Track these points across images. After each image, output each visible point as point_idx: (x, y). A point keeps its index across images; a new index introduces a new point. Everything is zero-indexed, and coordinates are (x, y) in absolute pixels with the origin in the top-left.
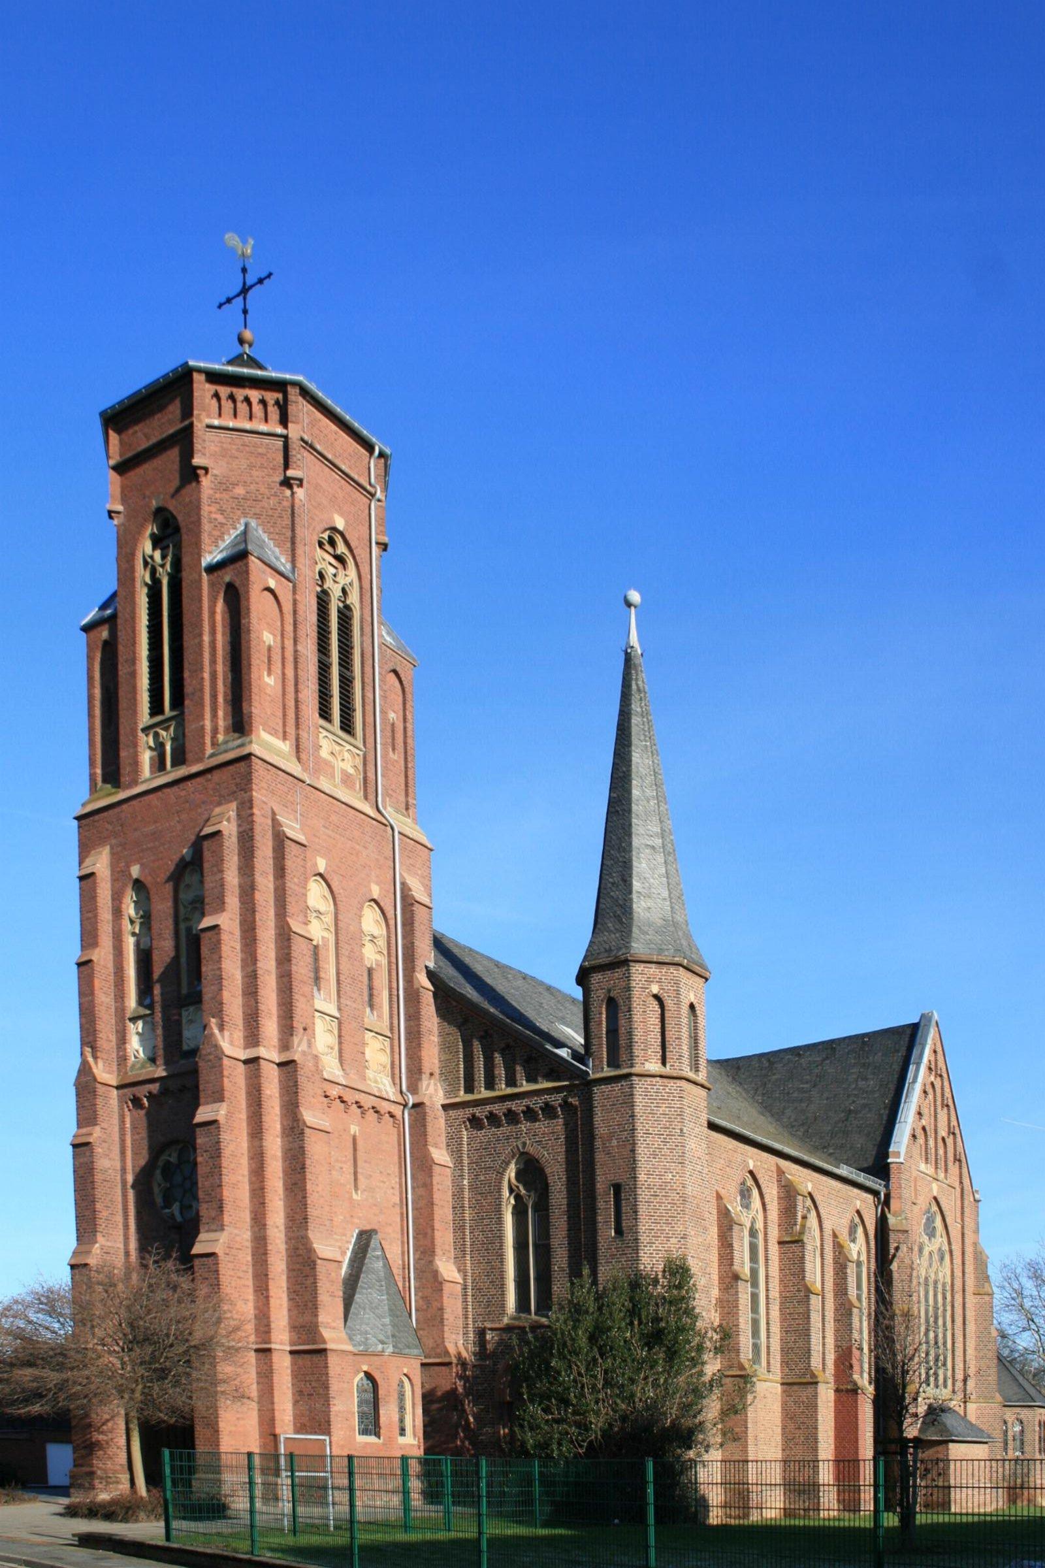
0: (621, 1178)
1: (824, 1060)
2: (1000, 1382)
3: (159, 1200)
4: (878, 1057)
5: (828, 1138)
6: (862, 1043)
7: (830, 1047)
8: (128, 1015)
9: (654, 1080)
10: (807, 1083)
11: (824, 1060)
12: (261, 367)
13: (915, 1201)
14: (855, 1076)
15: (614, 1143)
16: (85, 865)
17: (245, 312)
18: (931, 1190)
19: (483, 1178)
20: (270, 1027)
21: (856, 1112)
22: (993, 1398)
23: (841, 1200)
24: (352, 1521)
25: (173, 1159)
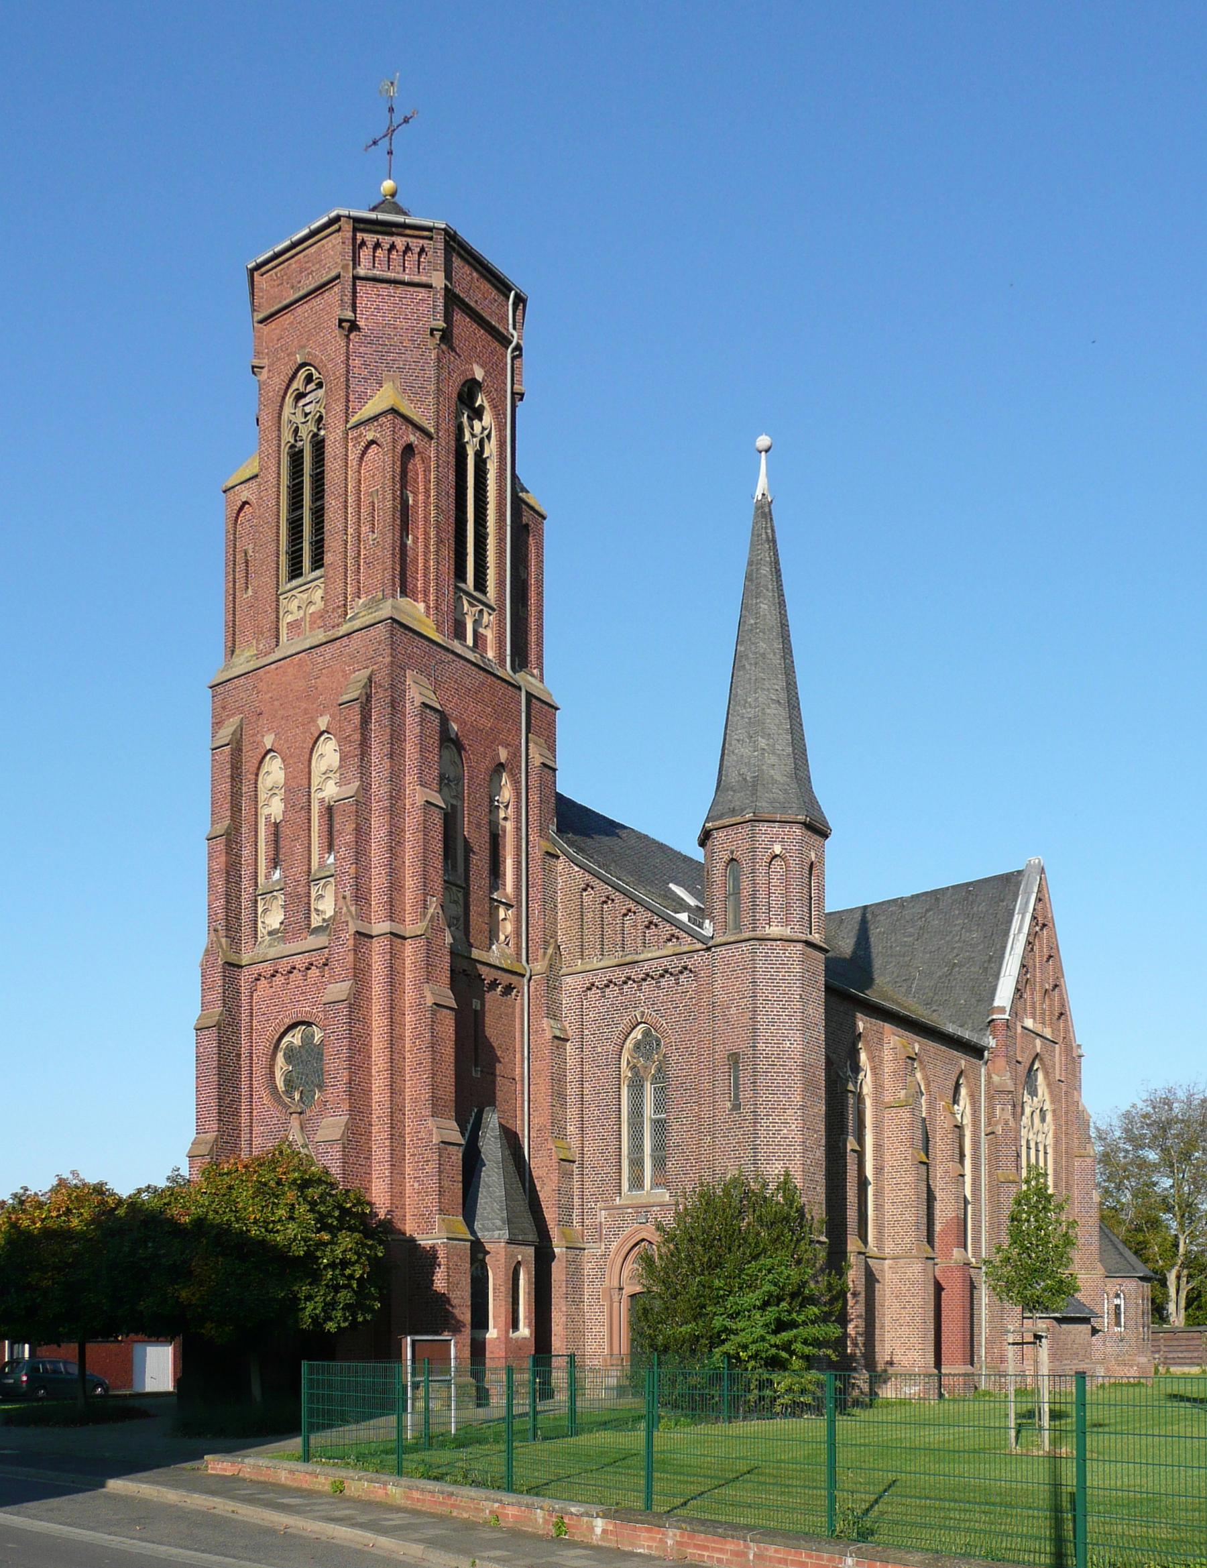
0: (743, 1047)
1: (928, 911)
2: (1102, 1251)
3: (280, 1083)
4: (983, 907)
5: (931, 995)
6: (967, 892)
7: (935, 896)
8: (514, 909)
9: (774, 943)
10: (910, 936)
11: (928, 911)
12: (405, 214)
13: (233, 958)
14: (958, 928)
15: (733, 1010)
16: (218, 736)
17: (390, 153)
18: (1035, 1046)
19: (600, 1050)
20: (377, 900)
21: (961, 965)
22: (1094, 1269)
23: (947, 1061)
24: (510, 1442)
25: (297, 1041)
